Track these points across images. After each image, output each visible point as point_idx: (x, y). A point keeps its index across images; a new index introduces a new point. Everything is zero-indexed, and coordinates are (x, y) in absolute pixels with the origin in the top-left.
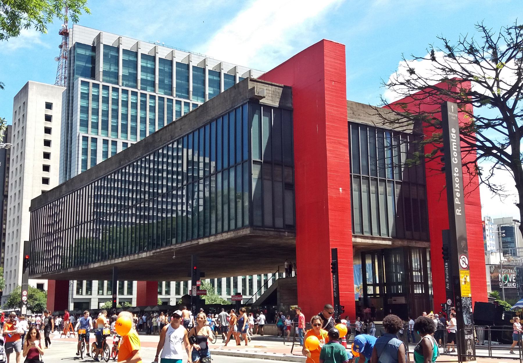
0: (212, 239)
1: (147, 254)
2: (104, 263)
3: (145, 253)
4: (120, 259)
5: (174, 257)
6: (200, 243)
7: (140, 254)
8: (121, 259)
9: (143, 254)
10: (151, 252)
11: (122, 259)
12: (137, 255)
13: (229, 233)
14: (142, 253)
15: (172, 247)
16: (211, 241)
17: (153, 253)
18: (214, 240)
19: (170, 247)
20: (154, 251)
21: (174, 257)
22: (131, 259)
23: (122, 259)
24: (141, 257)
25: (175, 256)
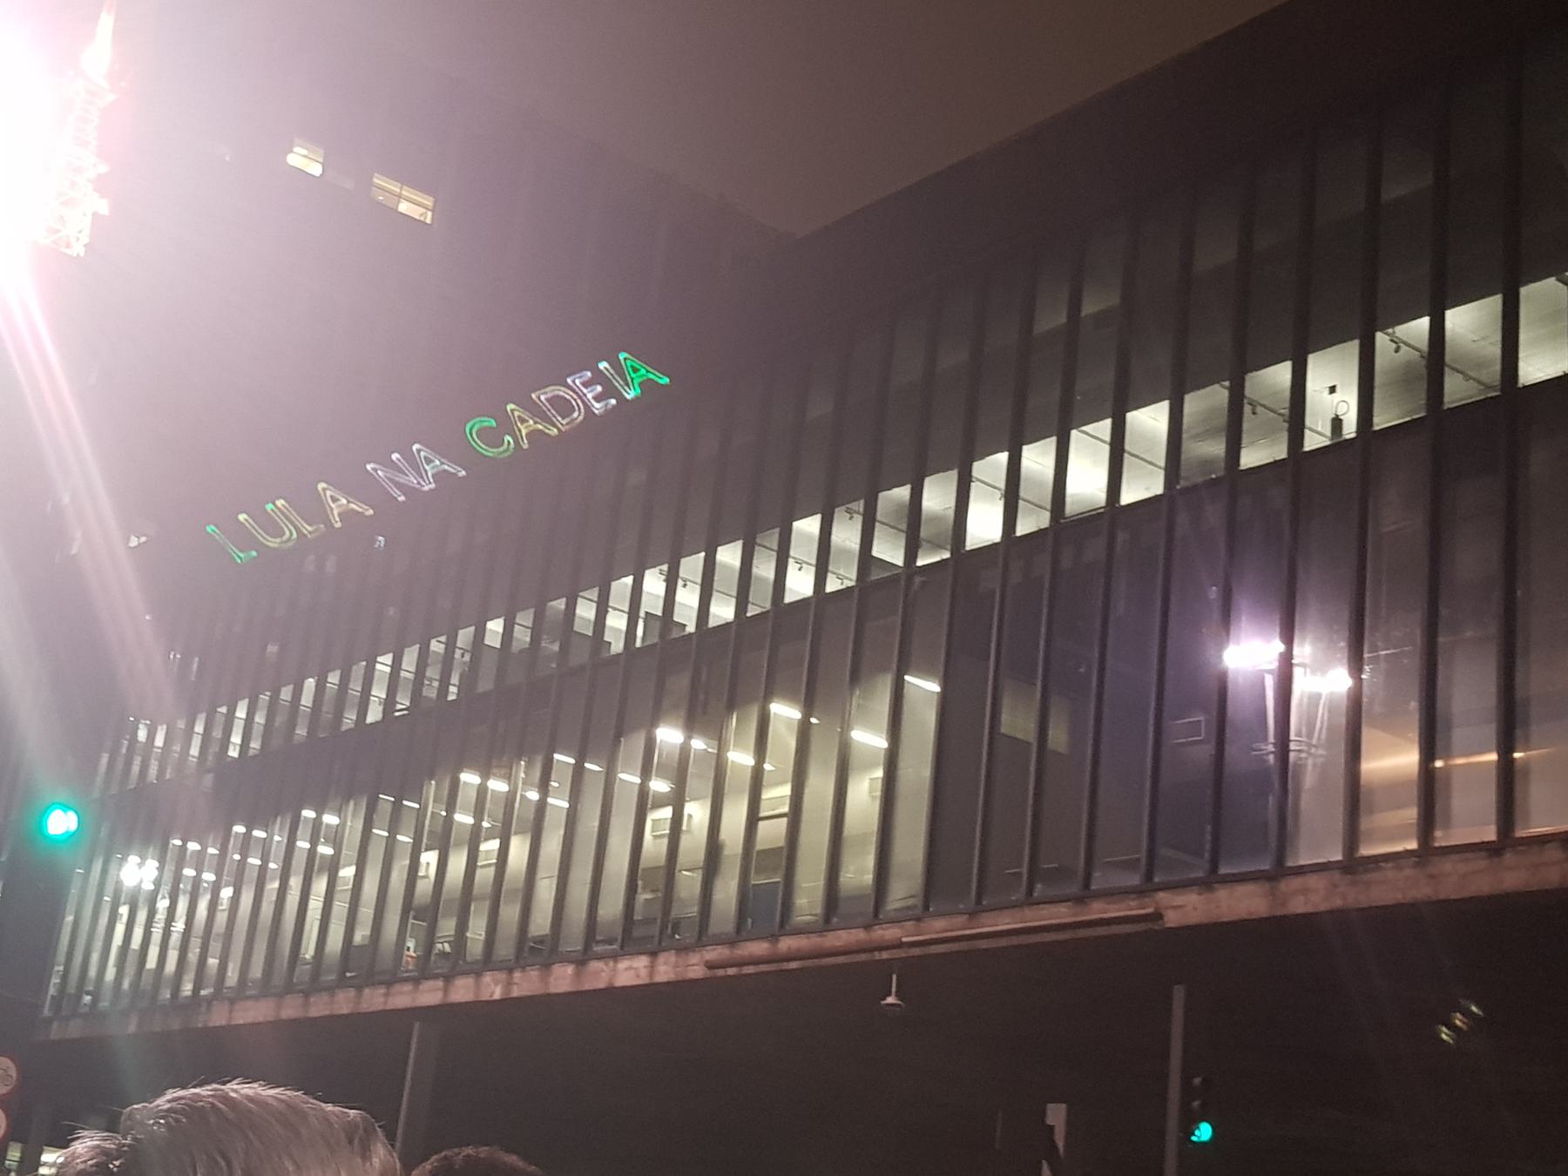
0: (1305, 891)
1: (652, 968)
2: (306, 1004)
3: (641, 962)
4: (427, 985)
5: (890, 1000)
6: (1172, 919)
7: (595, 965)
8: (440, 983)
9: (623, 964)
10: (694, 958)
11: (446, 990)
12: (570, 969)
13: (1509, 857)
14: (615, 957)
15: (787, 944)
16: (1298, 906)
17: (710, 966)
18: (1338, 903)
19: (867, 927)
20: (714, 953)
21: (890, 1000)
22: (516, 992)
23: (446, 990)
24: (601, 985)
25: (898, 995)
